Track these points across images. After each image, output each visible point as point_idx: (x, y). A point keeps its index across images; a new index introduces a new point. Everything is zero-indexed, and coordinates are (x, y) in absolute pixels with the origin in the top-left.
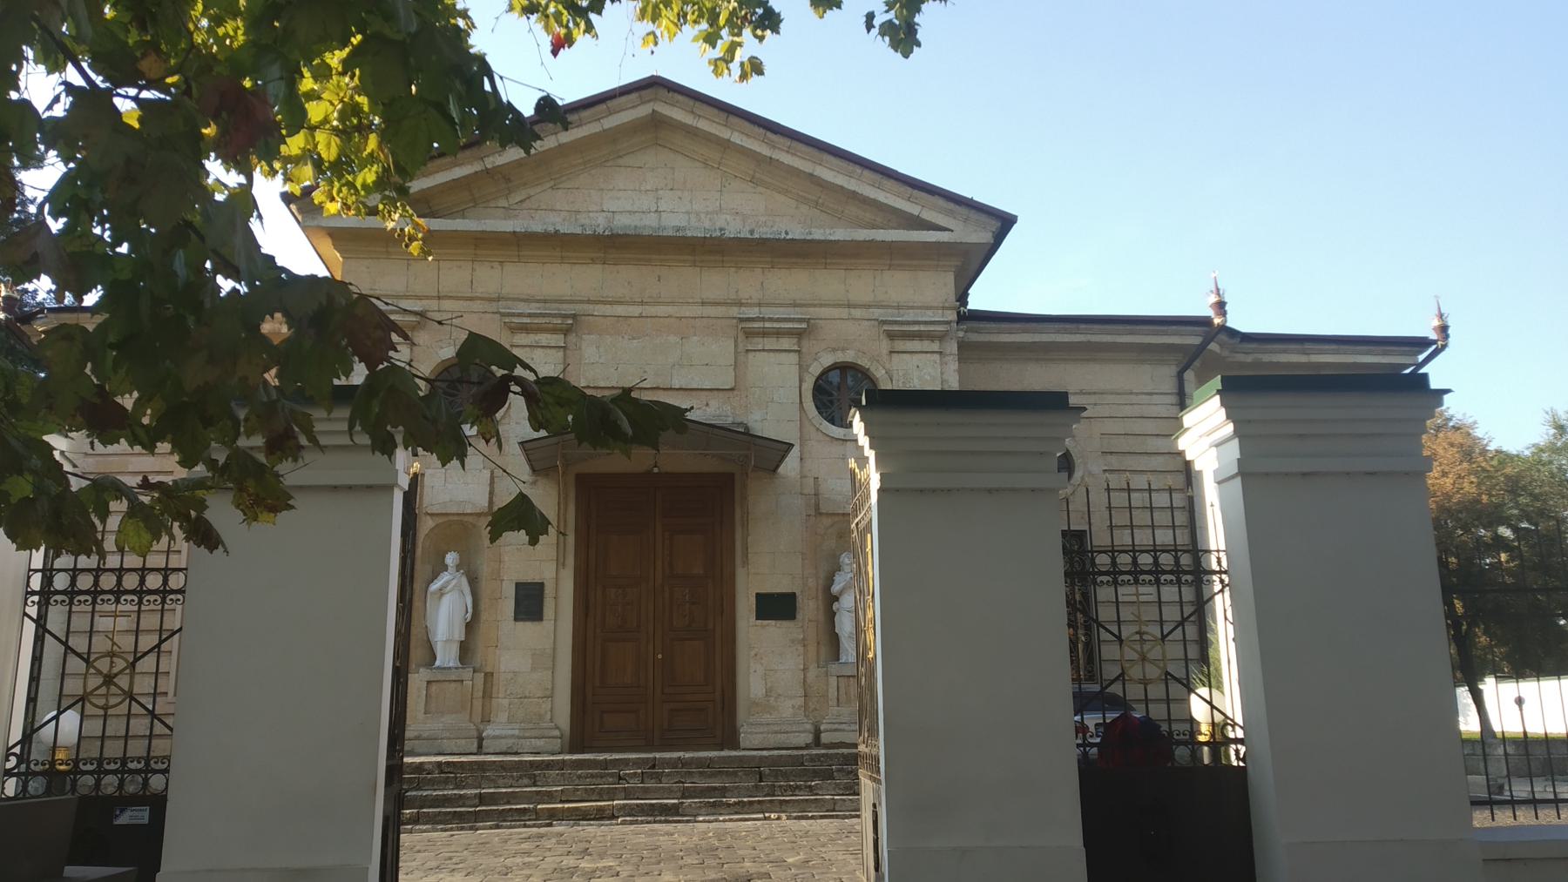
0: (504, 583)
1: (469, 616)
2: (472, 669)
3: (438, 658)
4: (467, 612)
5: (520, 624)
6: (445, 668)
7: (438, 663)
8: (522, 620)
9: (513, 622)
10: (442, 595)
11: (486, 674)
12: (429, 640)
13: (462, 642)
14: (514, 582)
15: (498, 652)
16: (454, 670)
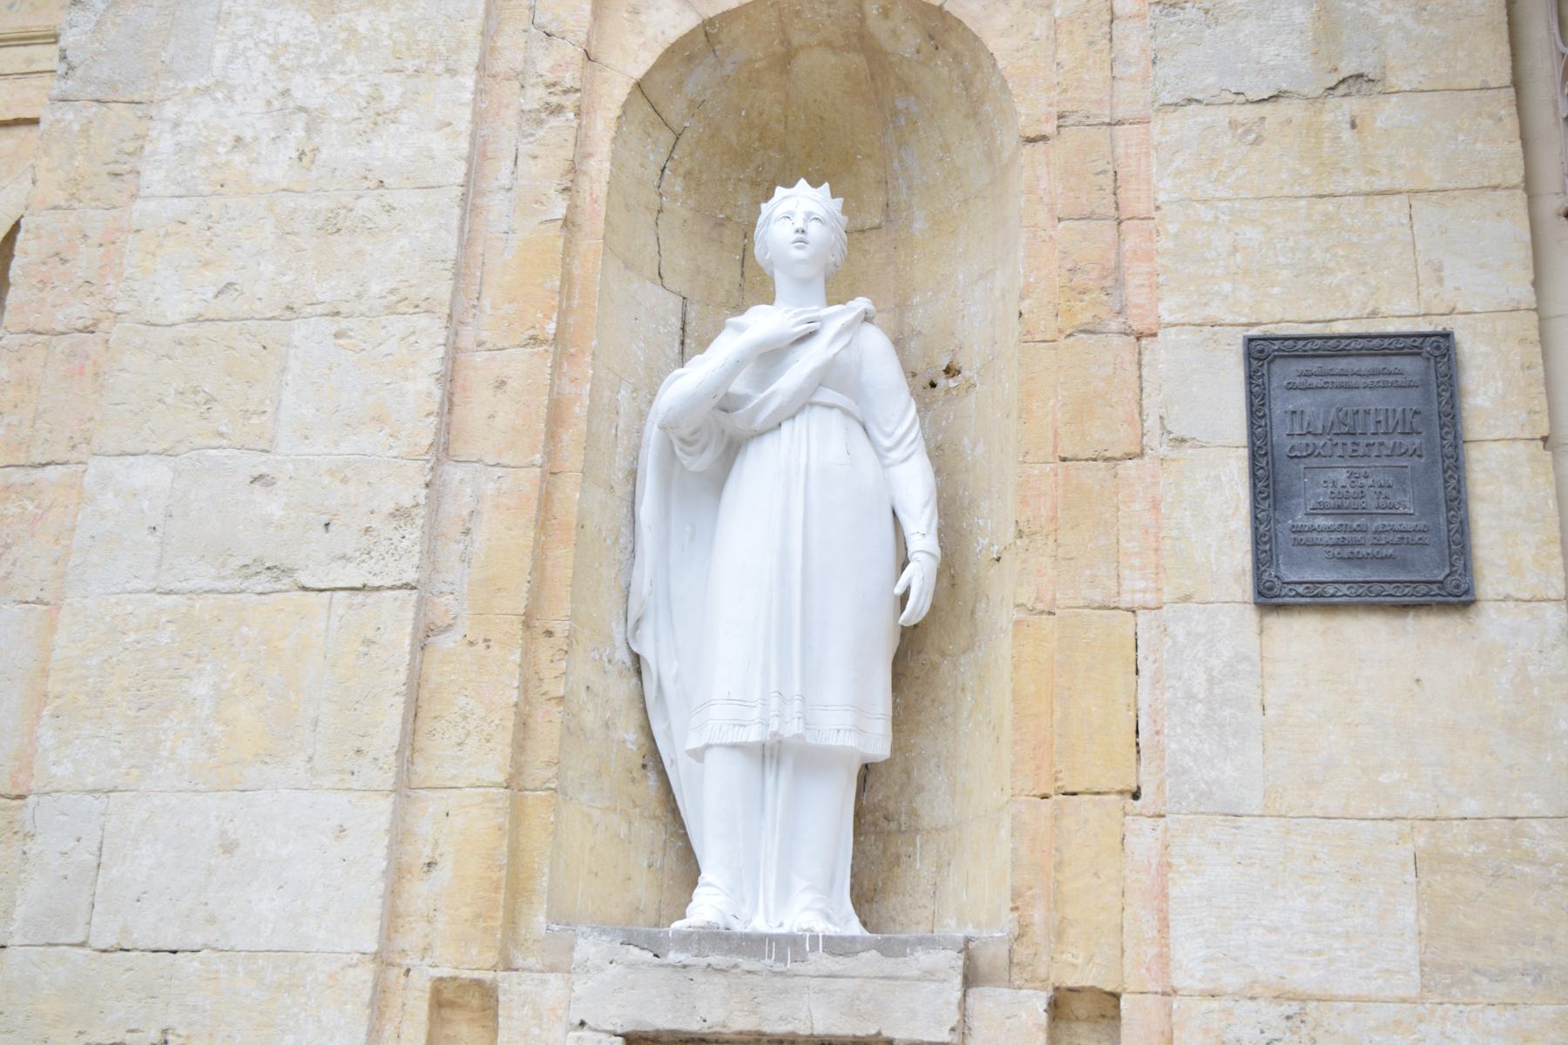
0: (1159, 354)
1: (920, 575)
2: (949, 961)
3: (706, 876)
4: (904, 564)
5: (1280, 625)
6: (754, 944)
7: (705, 908)
8: (1319, 601)
9: (1251, 613)
10: (733, 449)
11: (1060, 1006)
12: (653, 760)
13: (867, 774)
14: (1239, 336)
15: (1144, 838)
16: (821, 961)
